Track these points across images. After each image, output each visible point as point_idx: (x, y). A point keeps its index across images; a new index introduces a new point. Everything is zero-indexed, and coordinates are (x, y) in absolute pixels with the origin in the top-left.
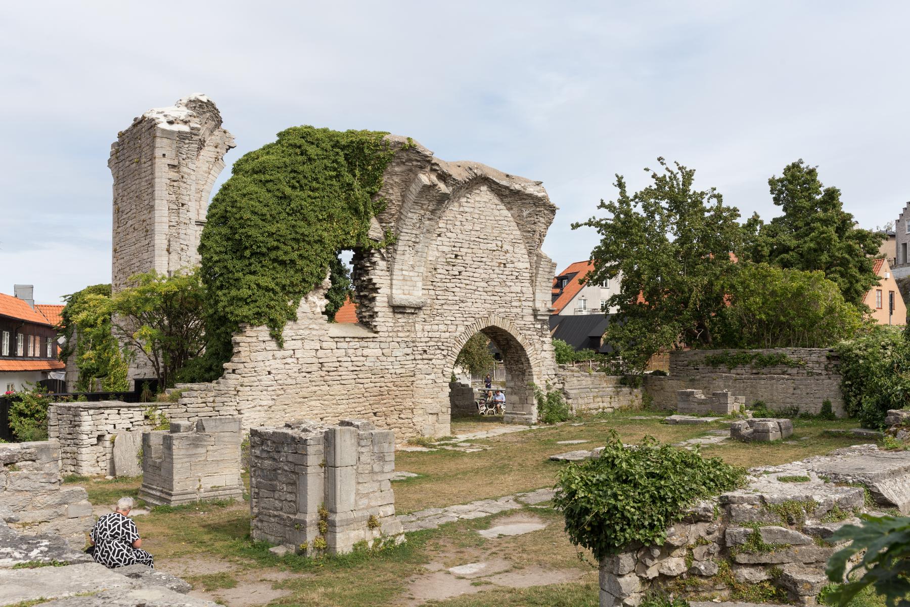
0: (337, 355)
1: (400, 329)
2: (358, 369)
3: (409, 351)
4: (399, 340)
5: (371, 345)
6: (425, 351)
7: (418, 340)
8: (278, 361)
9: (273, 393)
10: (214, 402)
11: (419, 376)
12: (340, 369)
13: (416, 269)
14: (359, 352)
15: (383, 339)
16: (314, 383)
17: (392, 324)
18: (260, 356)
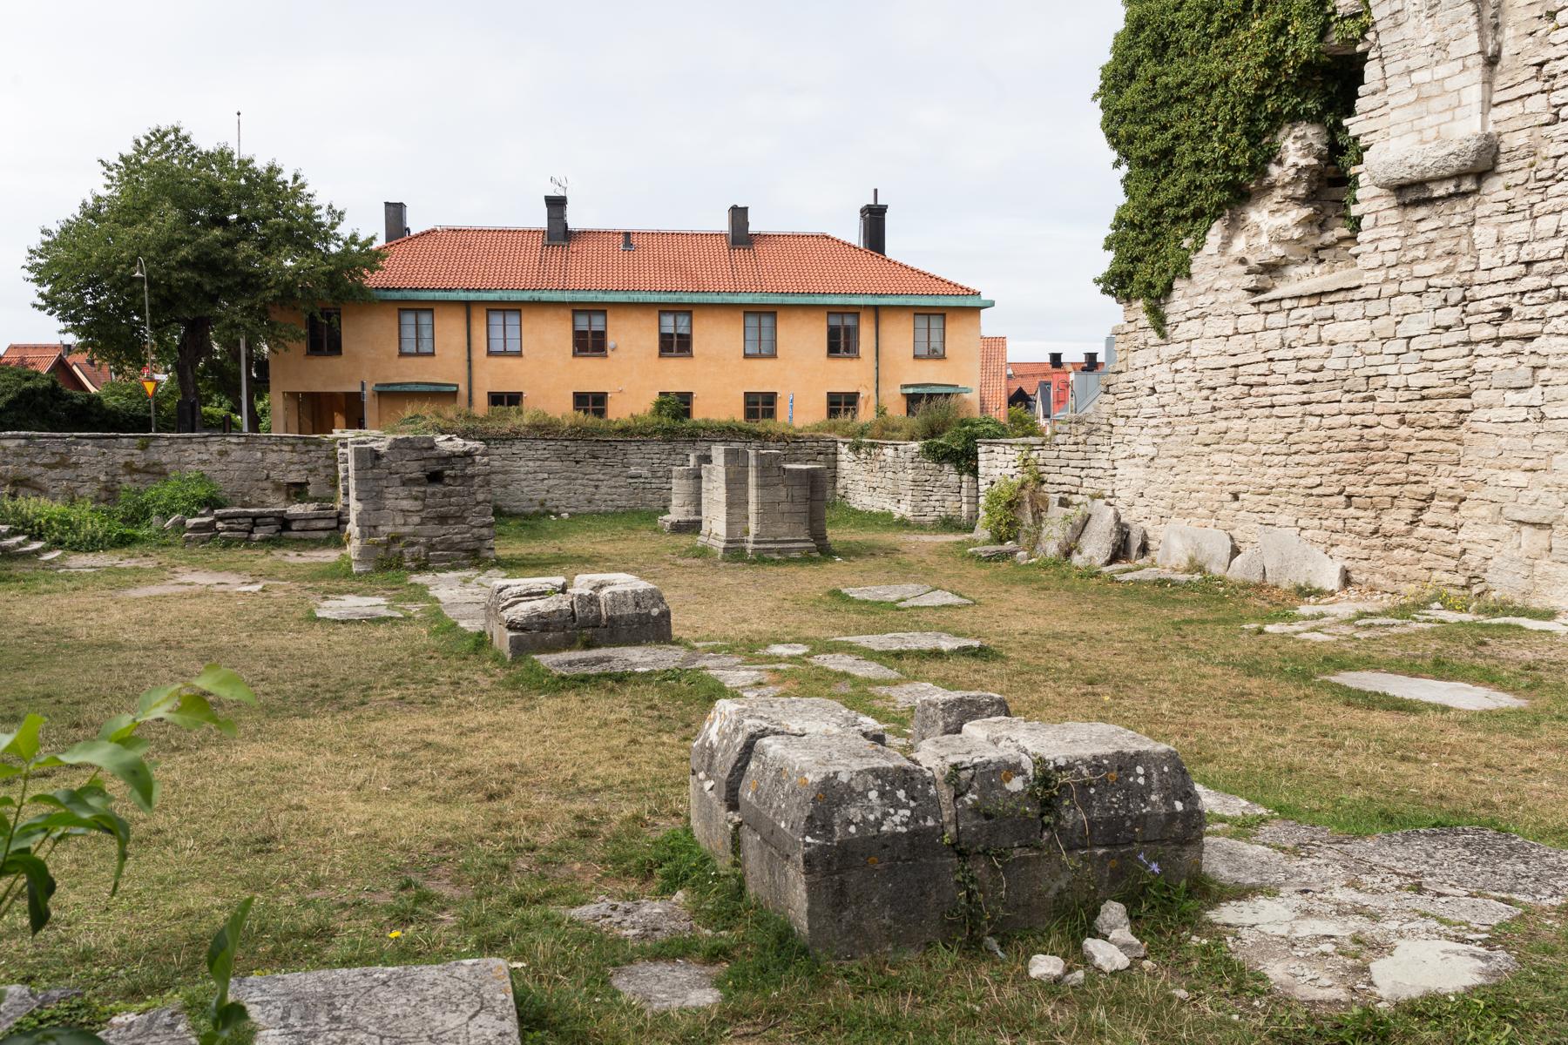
0: (1264, 345)
1: (1420, 252)
2: (1309, 377)
3: (1449, 316)
4: (1419, 285)
5: (1342, 311)
6: (1506, 312)
7: (1480, 276)
8: (1165, 366)
9: (1154, 431)
10: (1085, 443)
11: (1479, 397)
12: (1271, 379)
13: (1455, 50)
14: (1312, 334)
15: (1371, 292)
16: (1224, 414)
17: (1396, 244)
18: (1139, 359)
